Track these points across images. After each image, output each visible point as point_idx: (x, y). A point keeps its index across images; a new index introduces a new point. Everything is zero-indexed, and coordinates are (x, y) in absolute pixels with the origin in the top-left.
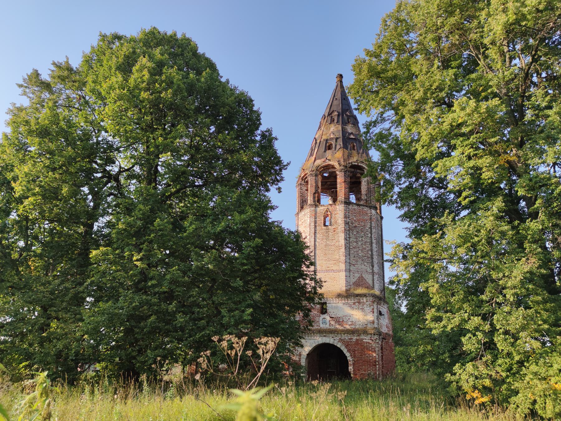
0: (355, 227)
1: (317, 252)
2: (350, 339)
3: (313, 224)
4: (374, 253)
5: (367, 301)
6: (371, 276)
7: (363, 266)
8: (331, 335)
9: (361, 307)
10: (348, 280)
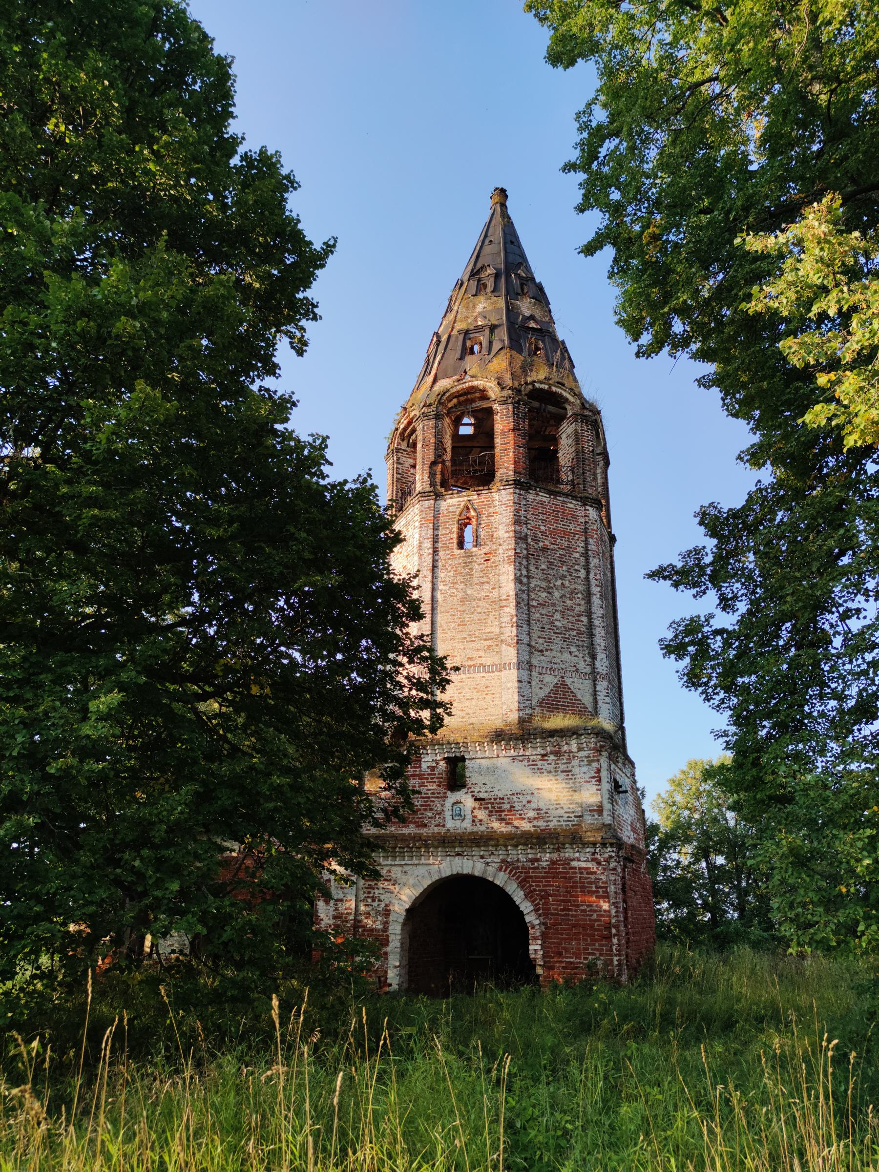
0: (544, 549)
1: (439, 618)
2: (533, 861)
3: (428, 544)
4: (596, 622)
5: (580, 749)
6: (588, 683)
7: (566, 655)
8: (476, 851)
9: (563, 767)
10: (526, 691)
